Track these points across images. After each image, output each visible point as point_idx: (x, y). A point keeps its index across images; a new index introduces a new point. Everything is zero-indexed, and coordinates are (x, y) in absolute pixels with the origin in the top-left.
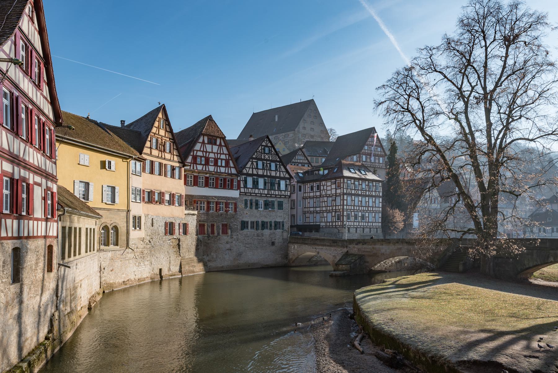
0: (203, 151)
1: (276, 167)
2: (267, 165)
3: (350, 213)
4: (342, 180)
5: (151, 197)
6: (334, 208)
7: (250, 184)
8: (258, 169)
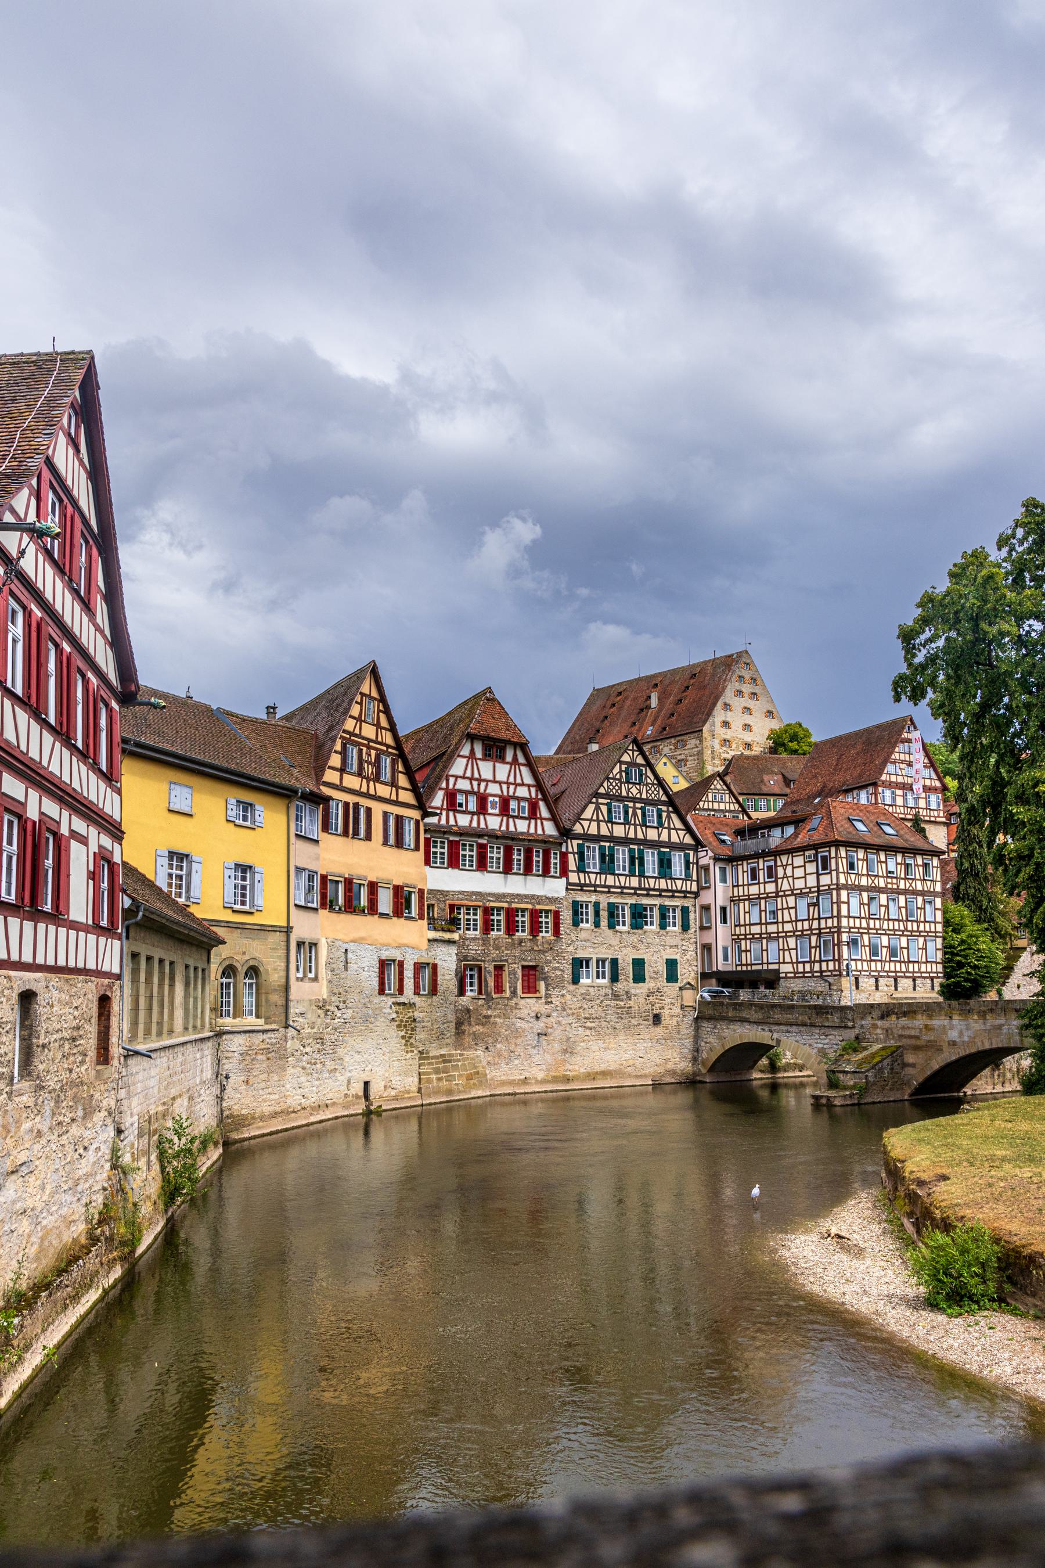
0: (471, 779)
1: (660, 816)
2: (635, 814)
4: (833, 850)
5: (345, 896)
6: (815, 925)
7: (594, 863)
8: (613, 823)
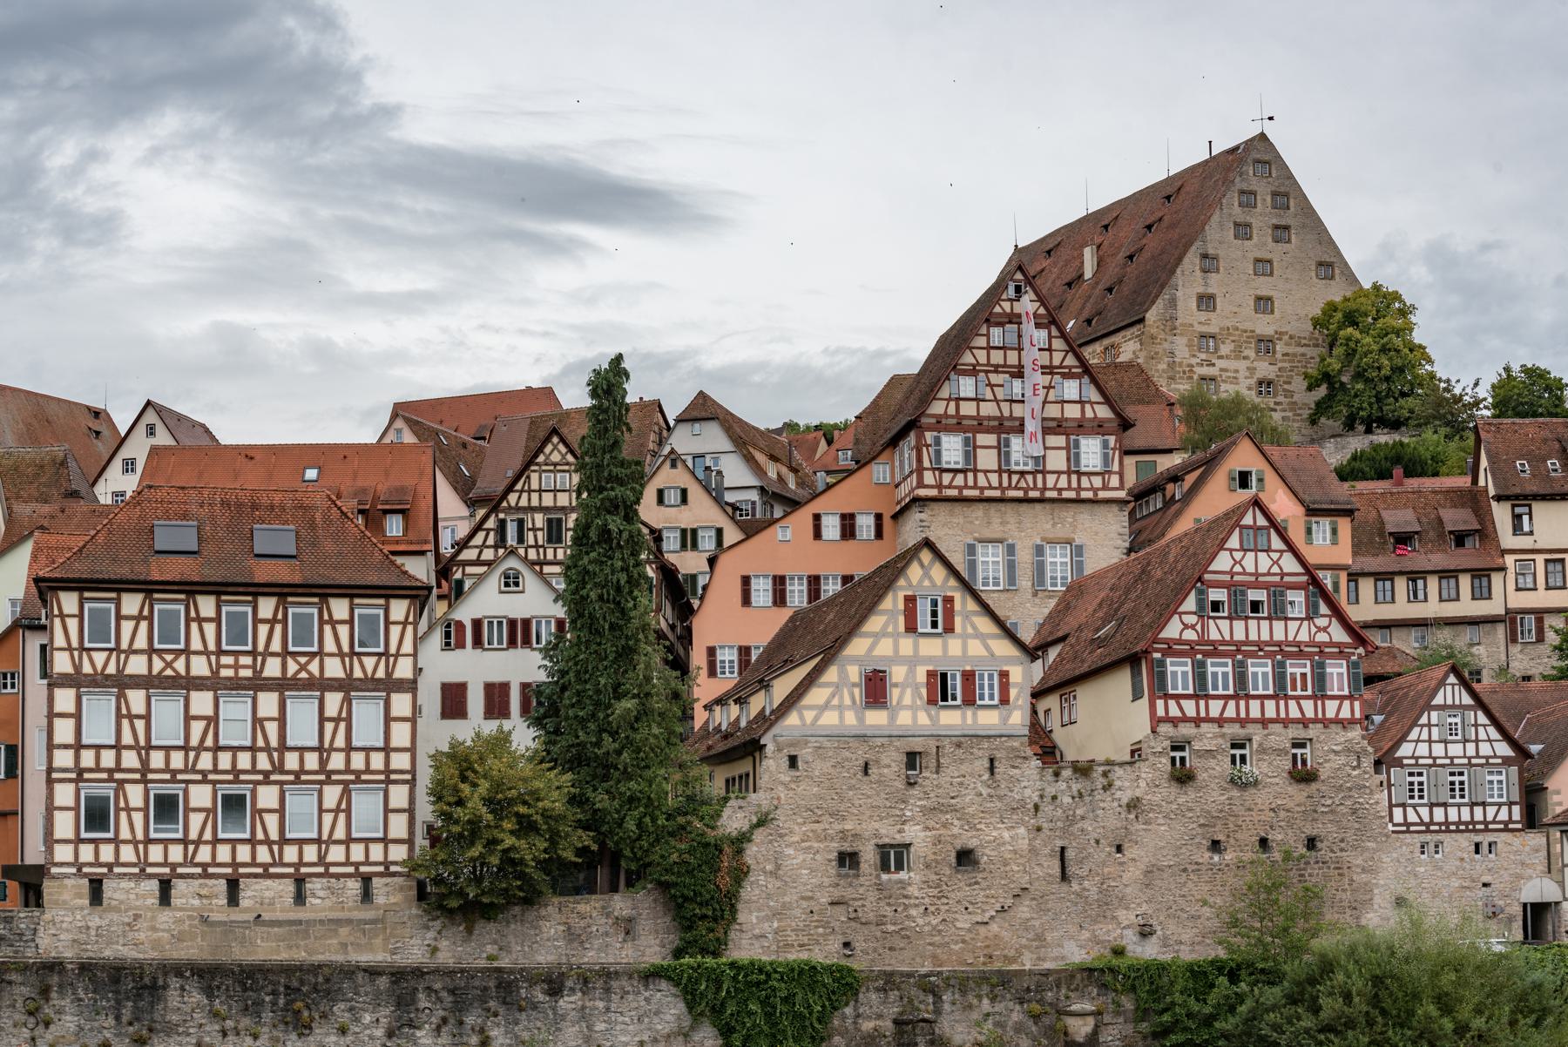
3: (108, 790)
